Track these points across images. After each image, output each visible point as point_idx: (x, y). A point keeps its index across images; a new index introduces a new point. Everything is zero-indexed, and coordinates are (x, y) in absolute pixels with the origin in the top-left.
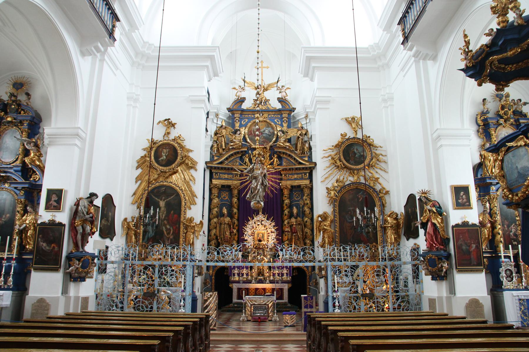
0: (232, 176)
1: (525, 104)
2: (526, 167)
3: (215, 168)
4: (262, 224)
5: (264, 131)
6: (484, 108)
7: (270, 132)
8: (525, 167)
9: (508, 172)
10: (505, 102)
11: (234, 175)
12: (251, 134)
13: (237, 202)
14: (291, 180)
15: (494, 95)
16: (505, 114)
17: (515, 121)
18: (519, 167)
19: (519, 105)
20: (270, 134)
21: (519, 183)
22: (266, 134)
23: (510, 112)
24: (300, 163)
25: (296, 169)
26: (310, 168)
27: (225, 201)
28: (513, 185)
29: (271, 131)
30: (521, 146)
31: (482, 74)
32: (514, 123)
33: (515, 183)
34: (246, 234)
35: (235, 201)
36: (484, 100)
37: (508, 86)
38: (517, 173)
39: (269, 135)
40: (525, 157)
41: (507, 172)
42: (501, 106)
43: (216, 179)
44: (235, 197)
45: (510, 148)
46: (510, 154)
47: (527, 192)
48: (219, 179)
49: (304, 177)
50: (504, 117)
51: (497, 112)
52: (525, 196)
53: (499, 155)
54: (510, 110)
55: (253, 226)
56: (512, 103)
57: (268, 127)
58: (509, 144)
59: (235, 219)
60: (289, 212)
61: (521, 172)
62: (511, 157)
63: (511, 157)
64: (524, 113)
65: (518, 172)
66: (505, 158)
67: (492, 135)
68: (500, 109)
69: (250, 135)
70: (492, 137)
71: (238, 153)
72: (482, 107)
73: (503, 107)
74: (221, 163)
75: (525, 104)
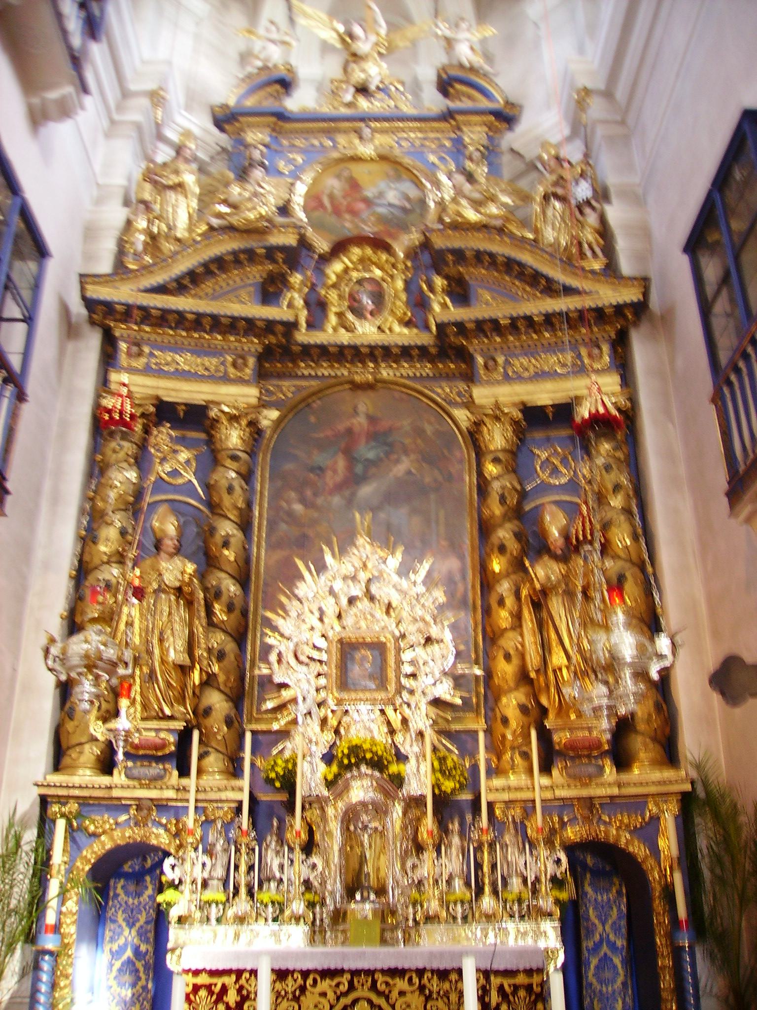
0: (214, 361)
3: (128, 313)
4: (372, 598)
5: (381, 195)
7: (408, 199)
11: (229, 359)
12: (321, 205)
13: (238, 484)
14: (519, 378)
20: (408, 206)
22: (390, 205)
24: (568, 291)
25: (549, 320)
26: (619, 309)
27: (177, 489)
29: (413, 193)
34: (280, 655)
35: (224, 484)
39: (404, 209)
43: (131, 370)
44: (228, 463)
48: (147, 371)
49: (586, 361)
55: (321, 610)
57: (398, 178)
59: (223, 575)
60: (518, 536)
69: (315, 209)
71: (251, 255)
74: (161, 289)
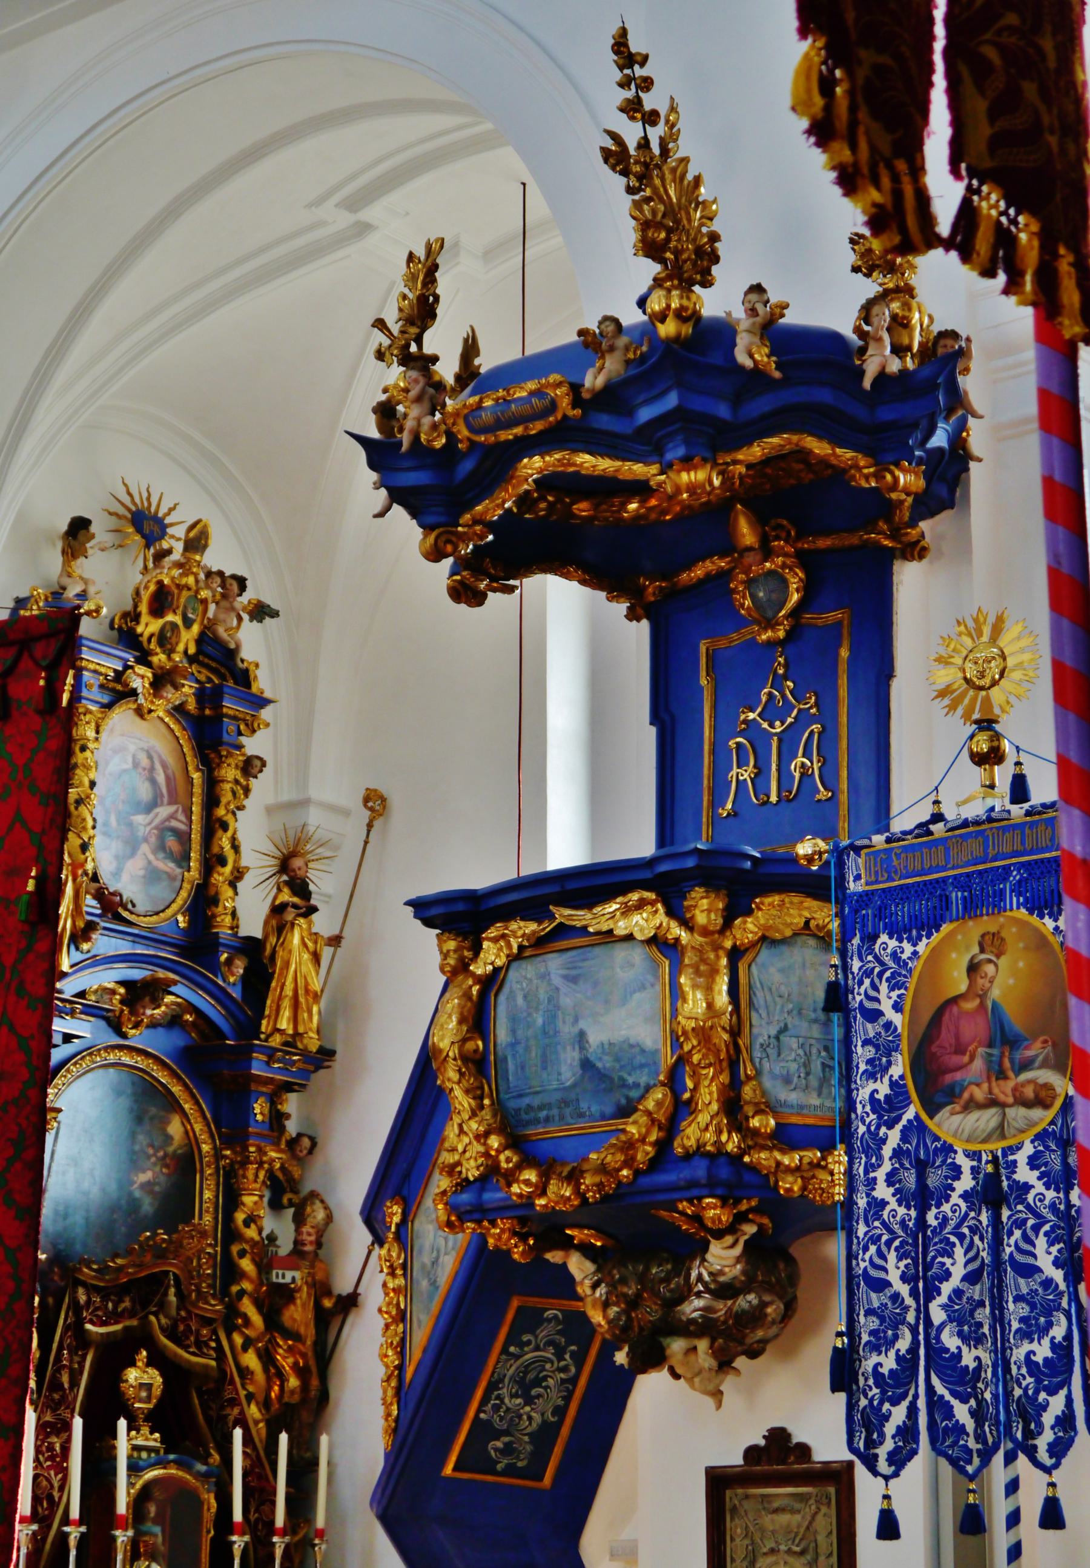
1: (261, 612)
2: (638, 1045)
6: (69, 576)
8: (632, 1046)
9: (520, 1049)
10: (176, 572)
15: (122, 511)
16: (165, 639)
17: (201, 695)
18: (596, 1038)
19: (233, 609)
21: (581, 1115)
23: (188, 639)
28: (536, 1122)
30: (630, 937)
31: (469, 506)
32: (192, 706)
33: (555, 1112)
36: (79, 527)
37: (511, 590)
38: (576, 1063)
40: (637, 996)
41: (513, 1045)
42: (152, 587)
45: (563, 931)
46: (554, 963)
47: (625, 1172)
50: (155, 660)
51: (125, 615)
52: (611, 1188)
53: (477, 949)
54: (188, 623)
56: (208, 587)
58: (563, 914)
61: (605, 1063)
62: (557, 981)
63: (557, 981)
64: (242, 661)
65: (586, 1064)
66: (513, 975)
67: (83, 749)
68: (143, 608)
70: (79, 757)
72: (53, 560)
73: (161, 602)
75: (261, 612)
